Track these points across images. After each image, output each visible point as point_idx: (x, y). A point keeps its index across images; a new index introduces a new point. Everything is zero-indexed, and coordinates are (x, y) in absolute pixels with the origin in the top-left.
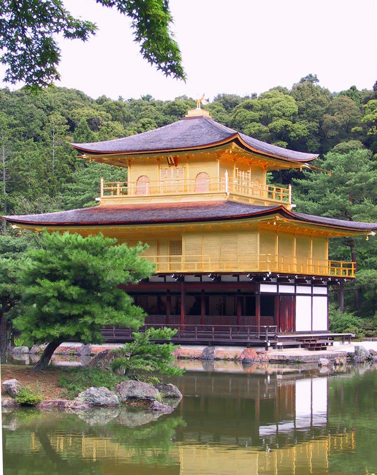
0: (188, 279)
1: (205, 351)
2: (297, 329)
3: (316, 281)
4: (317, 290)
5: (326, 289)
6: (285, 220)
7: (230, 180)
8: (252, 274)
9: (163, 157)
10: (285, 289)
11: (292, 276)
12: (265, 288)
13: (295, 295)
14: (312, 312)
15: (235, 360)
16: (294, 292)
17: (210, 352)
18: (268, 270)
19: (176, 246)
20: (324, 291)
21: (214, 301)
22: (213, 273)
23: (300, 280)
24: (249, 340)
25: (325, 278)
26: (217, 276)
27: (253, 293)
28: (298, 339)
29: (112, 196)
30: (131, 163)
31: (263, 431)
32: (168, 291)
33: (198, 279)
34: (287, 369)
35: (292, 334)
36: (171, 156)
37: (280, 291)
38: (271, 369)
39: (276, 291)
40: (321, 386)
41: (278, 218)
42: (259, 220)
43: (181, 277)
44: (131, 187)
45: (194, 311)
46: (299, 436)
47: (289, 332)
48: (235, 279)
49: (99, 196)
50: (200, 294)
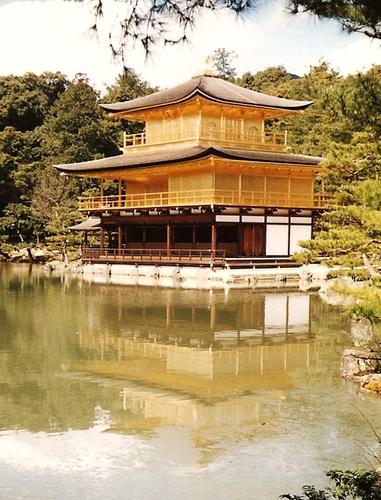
0: (172, 212)
3: (292, 213)
4: (294, 220)
8: (204, 207)
10: (246, 219)
11: (249, 208)
12: (219, 218)
13: (263, 226)
20: (309, 220)
23: (269, 212)
26: (186, 211)
28: (254, 261)
31: (218, 335)
41: (212, 158)
43: (165, 211)
46: (266, 341)
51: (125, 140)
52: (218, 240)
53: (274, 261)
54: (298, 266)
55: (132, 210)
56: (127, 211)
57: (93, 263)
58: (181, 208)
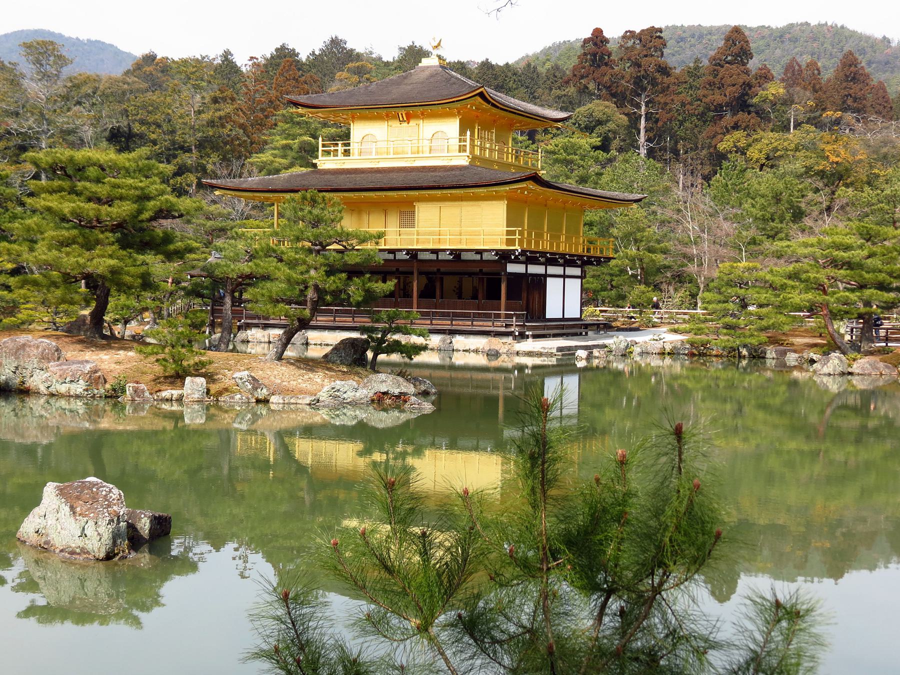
0: (422, 256)
1: (444, 341)
3: (569, 261)
4: (570, 271)
5: (580, 269)
6: (539, 188)
7: (472, 140)
8: (498, 252)
9: (393, 111)
10: (534, 269)
11: (543, 254)
12: (512, 268)
13: (546, 276)
14: (563, 297)
15: (476, 351)
16: (544, 272)
17: (449, 341)
18: (517, 247)
19: (408, 217)
20: (577, 271)
21: (450, 283)
22: (452, 250)
23: (552, 260)
24: (492, 329)
25: (580, 257)
26: (457, 254)
27: (499, 274)
29: (332, 158)
30: (354, 118)
32: (398, 270)
33: (434, 257)
34: (538, 361)
35: (542, 321)
36: (403, 112)
37: (529, 272)
39: (524, 272)
40: (572, 382)
42: (507, 188)
44: (354, 147)
45: (427, 294)
48: (478, 257)
49: (317, 157)
50: (435, 273)
51: (321, 148)
52: (508, 297)
53: (563, 327)
54: (581, 334)
57: (266, 327)
58: (452, 251)
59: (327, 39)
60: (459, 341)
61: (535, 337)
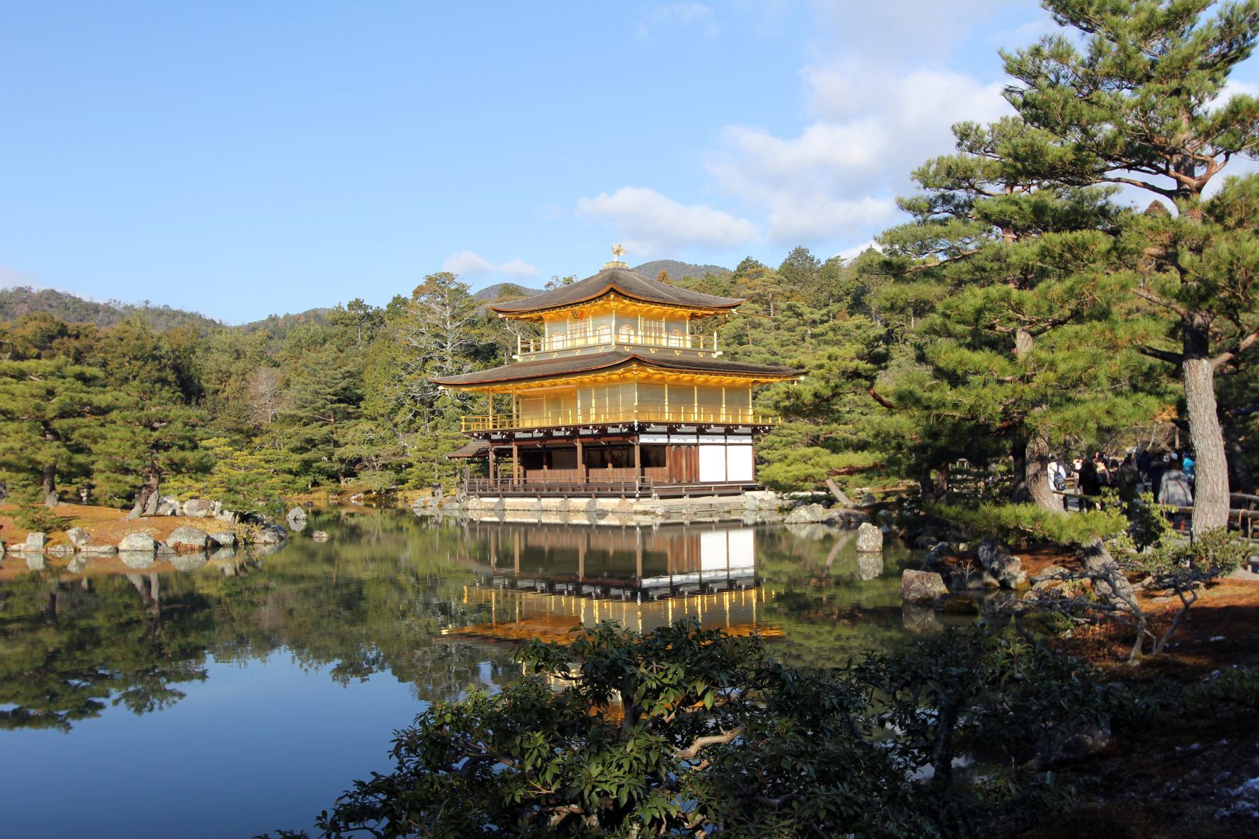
0: (582, 432)
2: (701, 480)
3: (729, 431)
4: (731, 440)
8: (624, 425)
12: (644, 439)
14: (727, 461)
20: (748, 440)
23: (701, 430)
26: (603, 430)
28: (687, 489)
31: (646, 582)
38: (645, 520)
43: (575, 431)
46: (704, 588)
47: (690, 482)
55: (531, 431)
56: (526, 431)
57: (481, 496)
59: (792, 250)
60: (604, 503)
61: (662, 497)
